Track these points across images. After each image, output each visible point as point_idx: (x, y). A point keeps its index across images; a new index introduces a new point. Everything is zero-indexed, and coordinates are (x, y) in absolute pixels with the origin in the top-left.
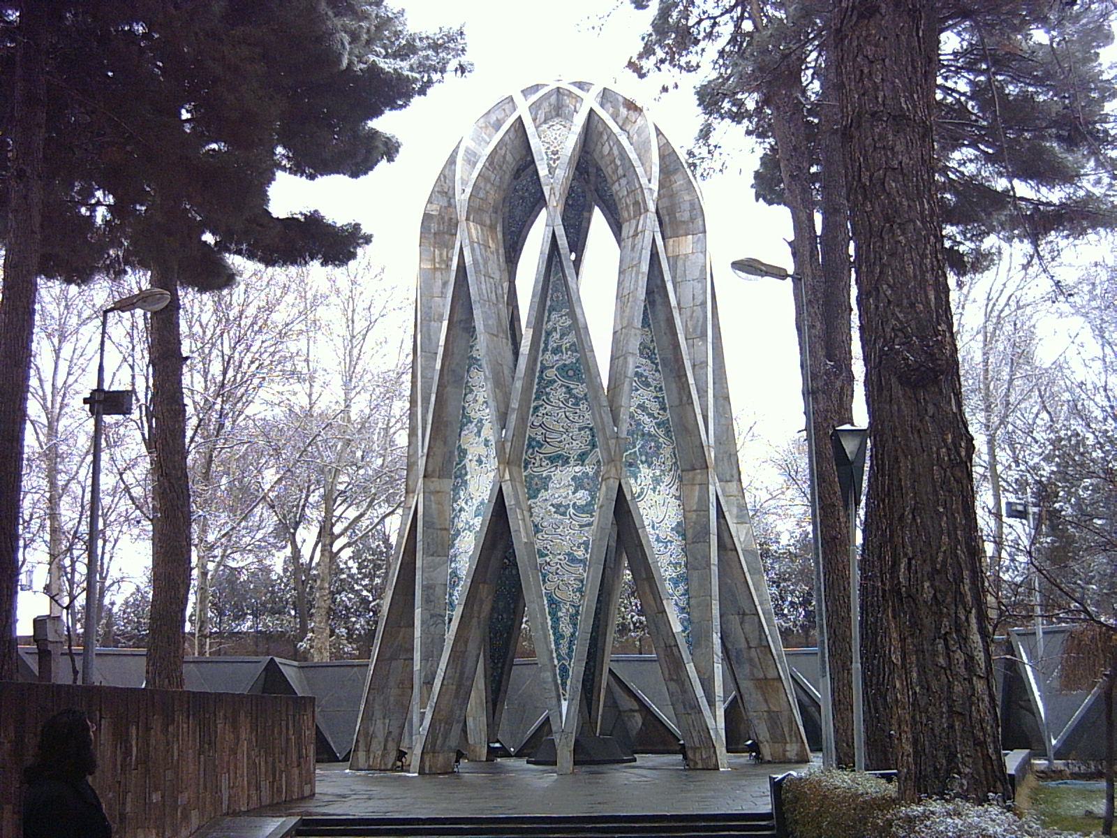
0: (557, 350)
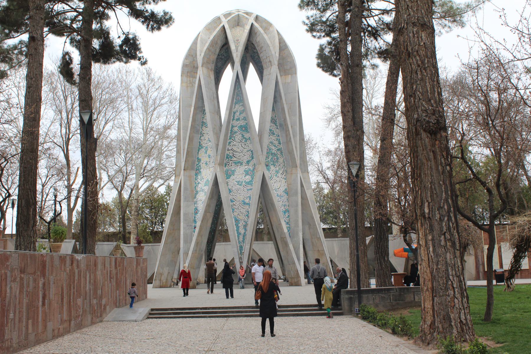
0: (238, 120)
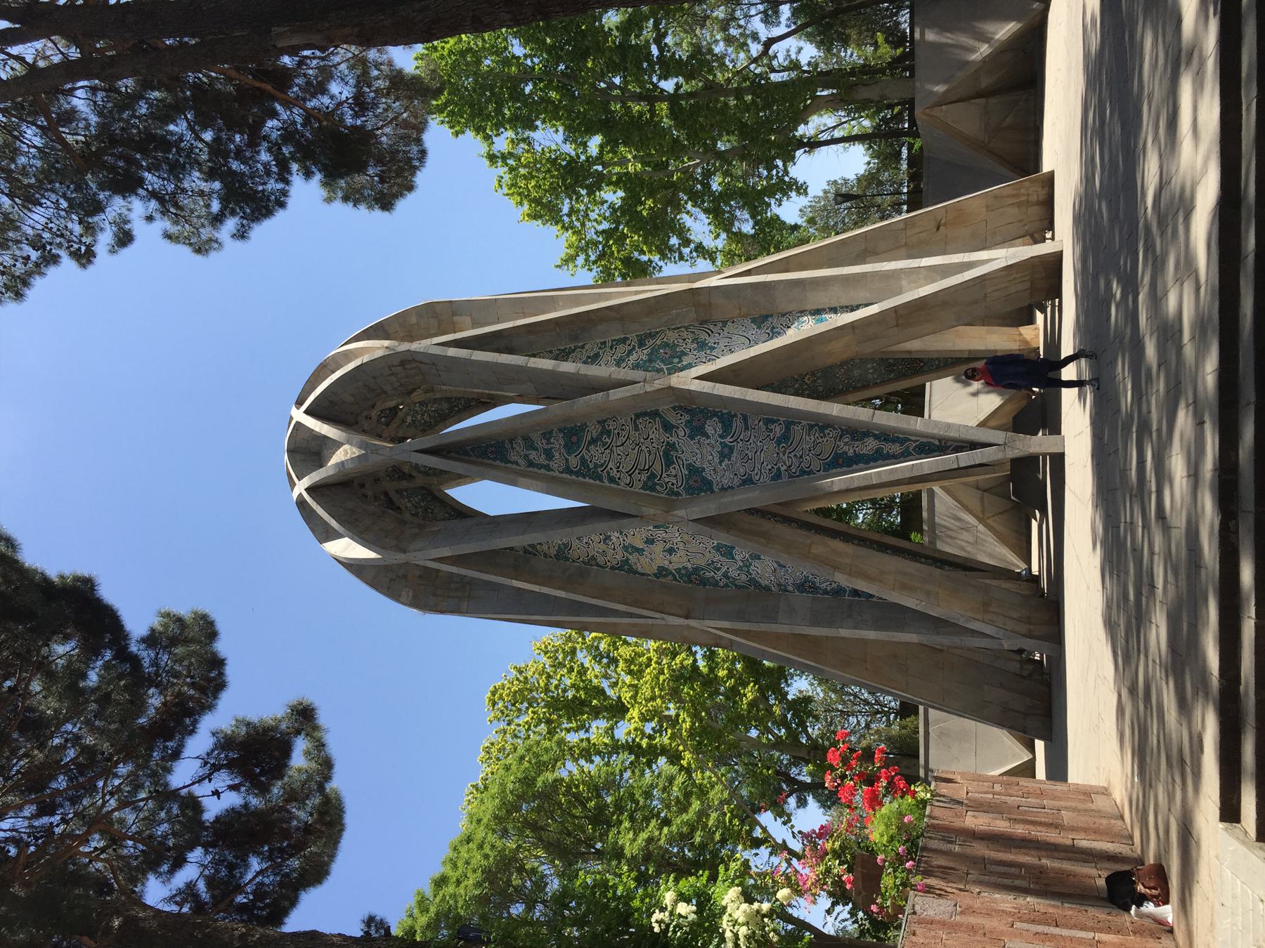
0: (549, 456)
